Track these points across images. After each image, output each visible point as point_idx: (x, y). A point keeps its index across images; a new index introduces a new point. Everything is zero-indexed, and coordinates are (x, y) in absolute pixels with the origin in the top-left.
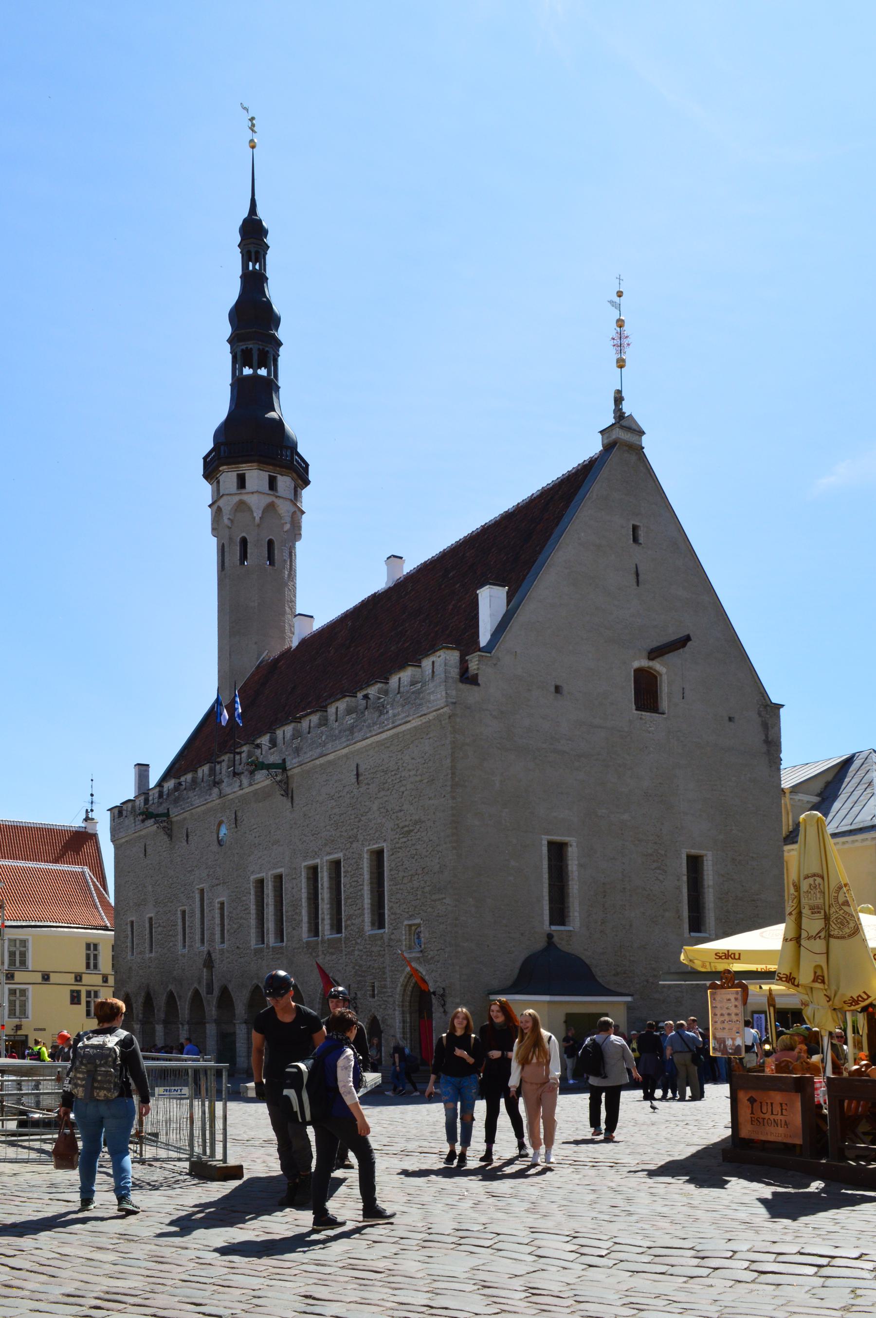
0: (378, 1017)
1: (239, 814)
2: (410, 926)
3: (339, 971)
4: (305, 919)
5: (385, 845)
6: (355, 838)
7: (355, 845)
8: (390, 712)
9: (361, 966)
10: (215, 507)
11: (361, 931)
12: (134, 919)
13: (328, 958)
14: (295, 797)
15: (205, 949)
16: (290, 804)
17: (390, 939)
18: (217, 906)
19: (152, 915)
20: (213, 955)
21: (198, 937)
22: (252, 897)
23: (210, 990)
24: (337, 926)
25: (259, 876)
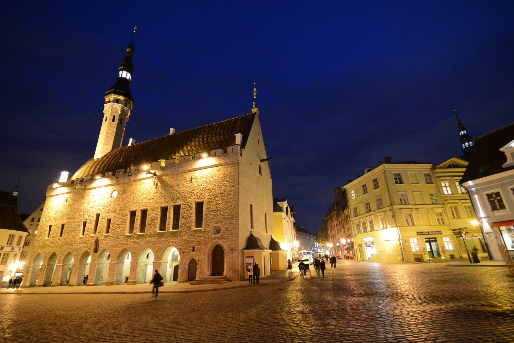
0: (196, 259)
11: (189, 229)
12: (52, 224)
13: (169, 238)
17: (205, 231)
24: (176, 225)
25: (133, 209)
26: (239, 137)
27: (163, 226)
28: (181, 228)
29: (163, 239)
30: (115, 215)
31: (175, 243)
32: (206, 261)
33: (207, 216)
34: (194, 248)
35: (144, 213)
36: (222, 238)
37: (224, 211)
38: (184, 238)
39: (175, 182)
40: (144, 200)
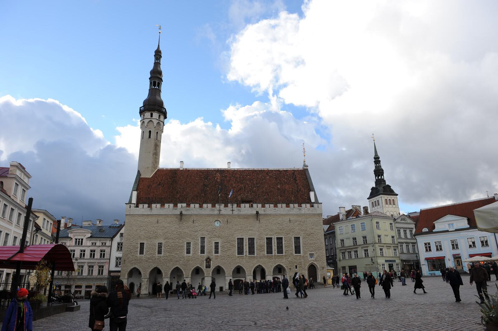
1: (229, 220)
2: (310, 254)
3: (282, 263)
4: (266, 250)
5: (301, 236)
6: (289, 234)
7: (289, 235)
8: (304, 211)
9: (292, 261)
10: (150, 120)
11: (292, 254)
13: (277, 260)
14: (260, 220)
15: (206, 255)
16: (259, 222)
18: (214, 243)
19: (163, 242)
20: (211, 257)
21: (200, 251)
22: (236, 242)
23: (208, 266)
26: (312, 194)
27: (269, 251)
28: (285, 253)
29: (272, 260)
30: (223, 240)
31: (282, 263)
32: (307, 273)
33: (303, 247)
34: (296, 266)
35: (251, 241)
36: (316, 261)
37: (316, 245)
38: (289, 260)
39: (276, 221)
40: (250, 231)
